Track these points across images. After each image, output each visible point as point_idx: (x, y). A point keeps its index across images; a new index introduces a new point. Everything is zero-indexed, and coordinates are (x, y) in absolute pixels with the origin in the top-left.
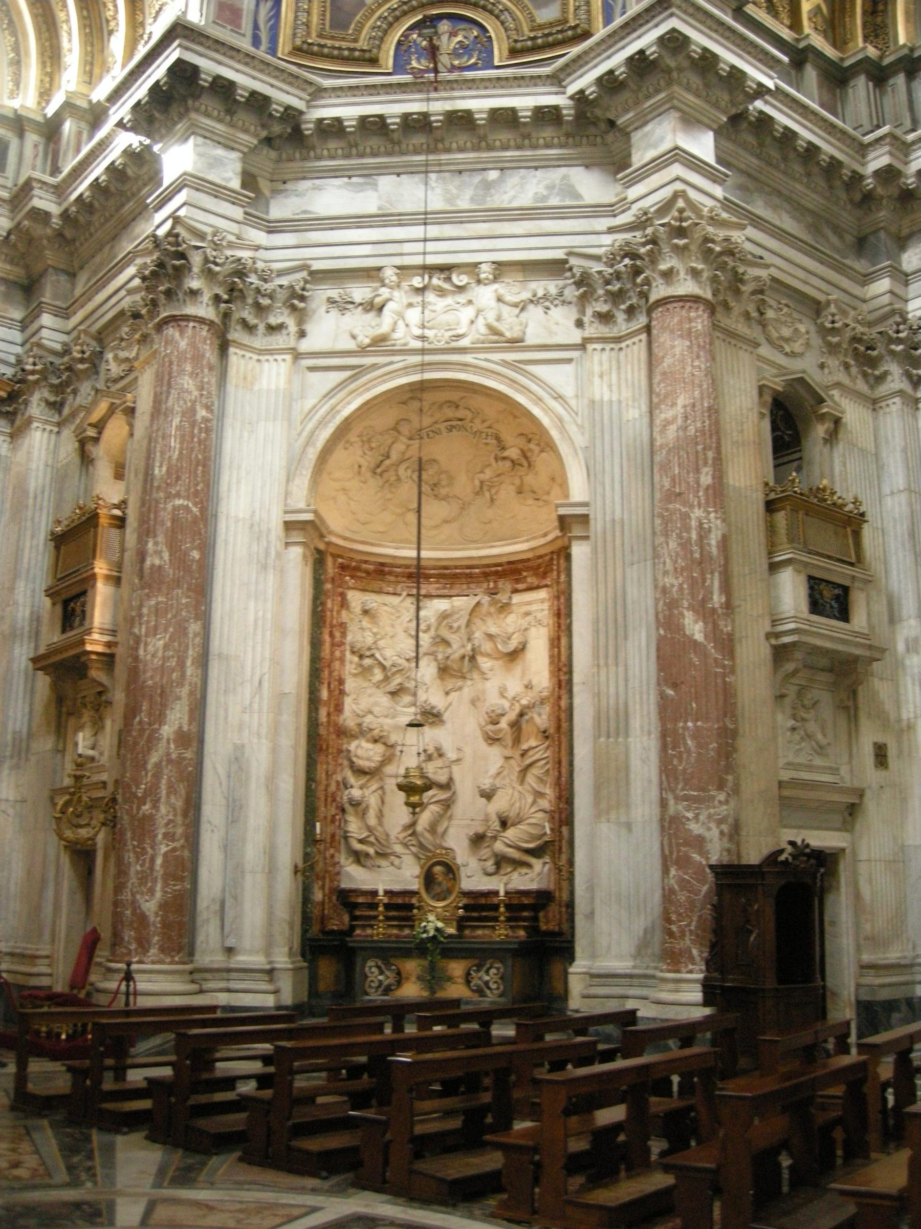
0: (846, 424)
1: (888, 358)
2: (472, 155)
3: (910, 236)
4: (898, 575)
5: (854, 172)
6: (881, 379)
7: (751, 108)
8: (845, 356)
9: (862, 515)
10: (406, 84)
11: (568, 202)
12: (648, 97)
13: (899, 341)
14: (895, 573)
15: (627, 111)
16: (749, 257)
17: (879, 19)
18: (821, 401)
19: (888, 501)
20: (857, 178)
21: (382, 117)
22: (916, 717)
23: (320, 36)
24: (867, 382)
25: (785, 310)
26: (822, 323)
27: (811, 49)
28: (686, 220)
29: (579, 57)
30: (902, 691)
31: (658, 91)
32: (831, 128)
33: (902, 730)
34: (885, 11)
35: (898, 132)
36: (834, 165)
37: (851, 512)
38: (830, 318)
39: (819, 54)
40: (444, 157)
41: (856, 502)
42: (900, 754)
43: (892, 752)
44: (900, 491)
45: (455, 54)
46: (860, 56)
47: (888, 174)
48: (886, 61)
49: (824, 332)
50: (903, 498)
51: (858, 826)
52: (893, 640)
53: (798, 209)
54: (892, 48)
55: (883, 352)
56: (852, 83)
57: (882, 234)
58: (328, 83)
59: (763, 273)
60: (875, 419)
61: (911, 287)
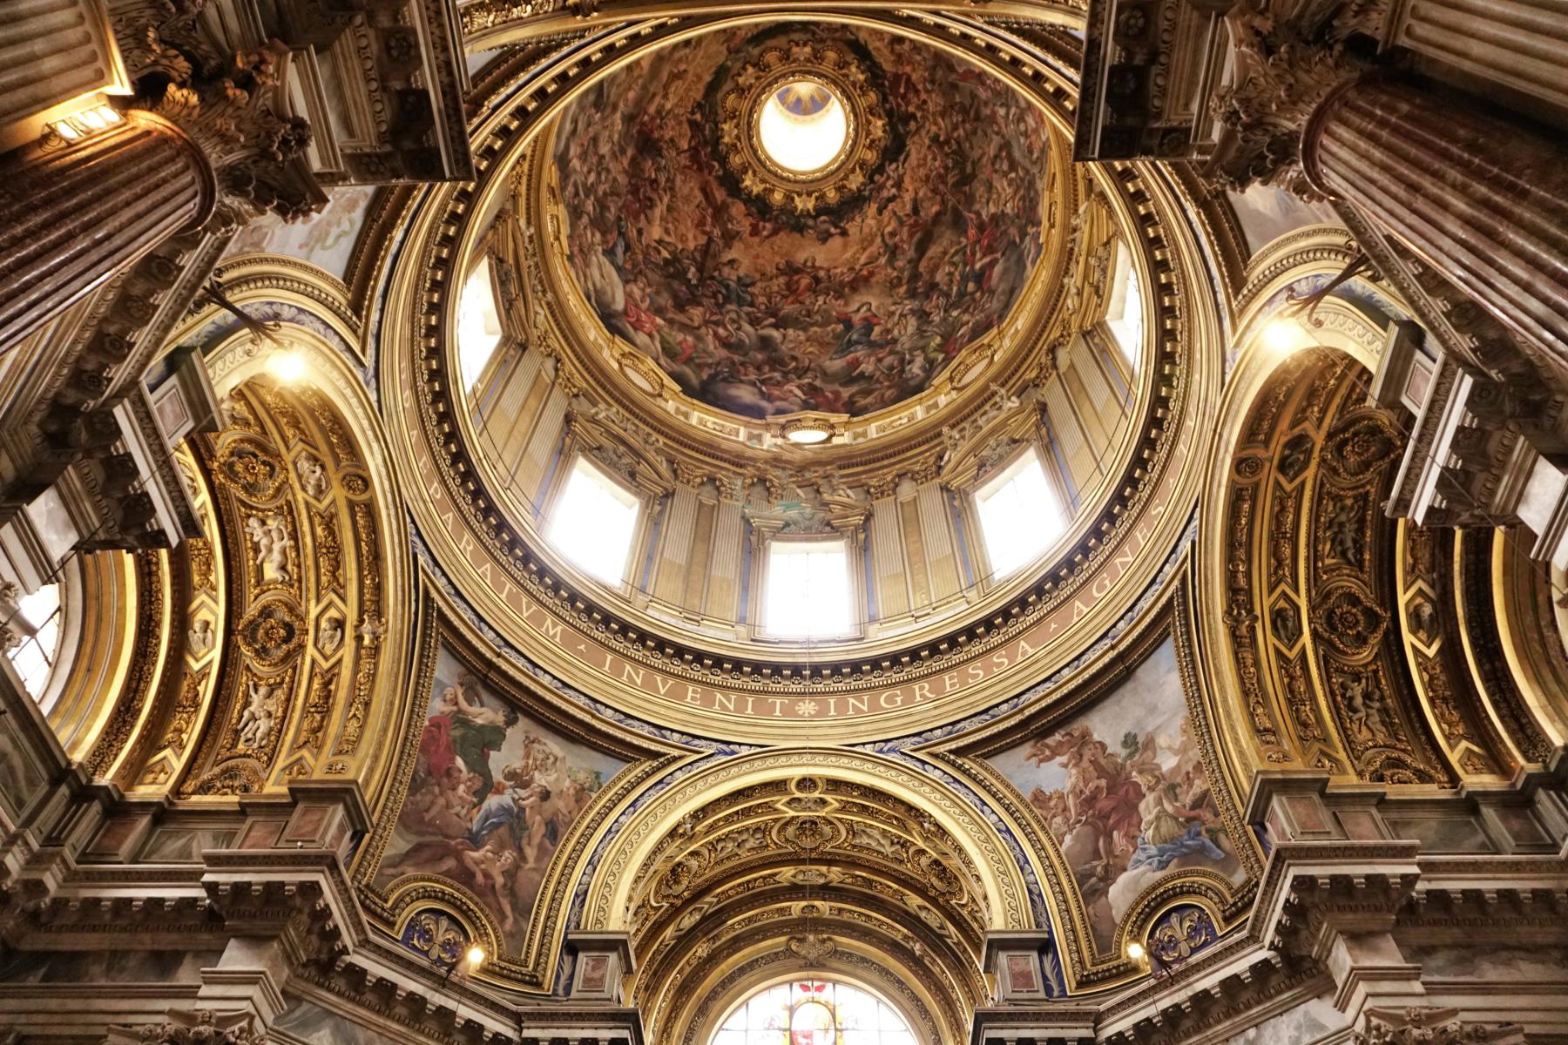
2: (1228, 1023)
10: (1153, 987)
11: (1318, 1037)
12: (1318, 930)
15: (1312, 945)
21: (1148, 1020)
23: (1094, 965)
28: (1386, 1035)
29: (1256, 918)
31: (1321, 924)
39: (1486, 795)
40: (1209, 1033)
45: (1190, 937)
48: (1552, 767)
58: (1102, 1008)
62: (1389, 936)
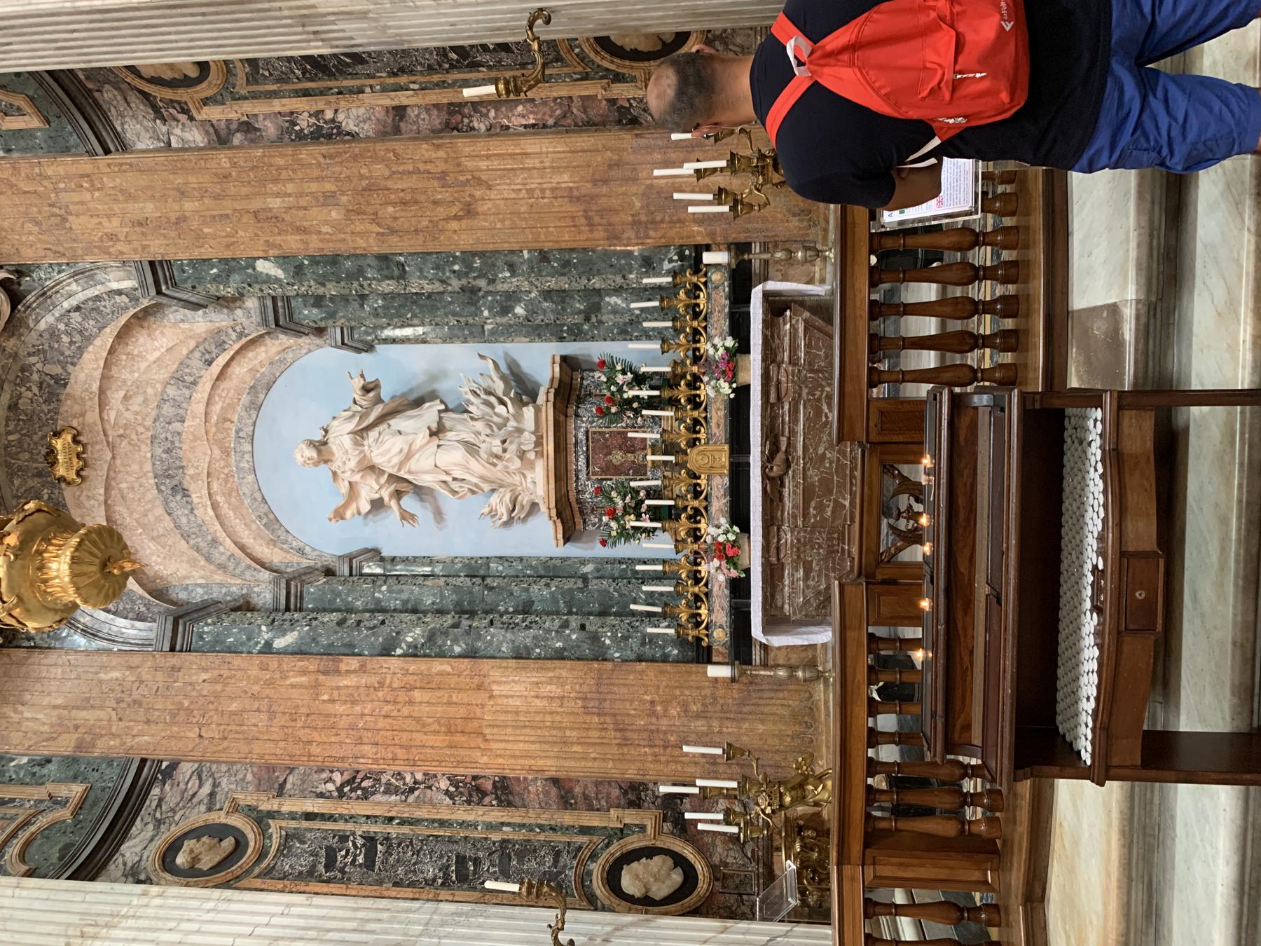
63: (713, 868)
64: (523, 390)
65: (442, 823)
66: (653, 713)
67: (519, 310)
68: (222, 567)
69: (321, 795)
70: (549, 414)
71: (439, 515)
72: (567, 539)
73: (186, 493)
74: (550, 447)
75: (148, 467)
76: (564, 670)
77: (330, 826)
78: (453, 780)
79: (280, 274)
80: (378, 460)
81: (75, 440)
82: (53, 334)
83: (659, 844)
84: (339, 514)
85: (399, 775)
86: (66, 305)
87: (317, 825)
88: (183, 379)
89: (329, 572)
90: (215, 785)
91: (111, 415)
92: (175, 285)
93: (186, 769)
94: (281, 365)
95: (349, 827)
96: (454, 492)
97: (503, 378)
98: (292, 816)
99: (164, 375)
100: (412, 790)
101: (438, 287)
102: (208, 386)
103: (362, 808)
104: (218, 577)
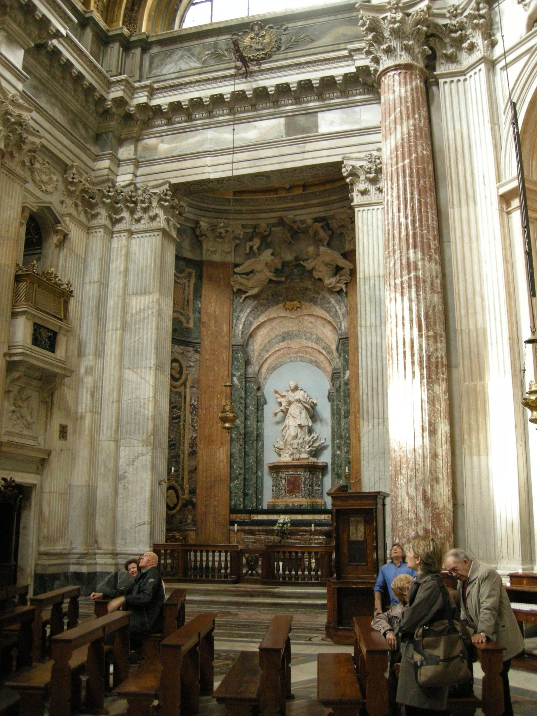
0: (70, 238)
1: (101, 206)
3: (126, 140)
4: (87, 330)
5: (102, 95)
6: (95, 216)
7: (50, 43)
8: (77, 199)
9: (71, 292)
13: (109, 197)
14: (85, 328)
16: (31, 129)
17: (134, 14)
18: (58, 222)
19: (87, 287)
20: (102, 99)
22: (86, 412)
24: (86, 217)
25: (47, 165)
26: (67, 178)
27: (92, 19)
30: (80, 396)
32: (94, 68)
33: (77, 419)
34: (138, 11)
35: (131, 80)
36: (91, 89)
37: (65, 289)
38: (72, 175)
39: (96, 24)
41: (69, 284)
42: (75, 431)
43: (70, 431)
44: (95, 282)
46: (119, 32)
47: (120, 102)
48: (132, 39)
49: (67, 183)
50: (96, 286)
51: (45, 472)
52: (79, 366)
53: (65, 108)
54: (137, 32)
55: (99, 201)
56: (111, 45)
57: (110, 135)
59: (37, 141)
60: (88, 238)
61: (121, 168)
62: (23, 51)
63: (174, 515)
64: (316, 453)
65: (184, 437)
66: (215, 496)
67: (338, 452)
68: (259, 354)
69: (191, 399)
70: (304, 462)
71: (278, 423)
72: (269, 467)
73: (283, 341)
74: (295, 463)
75: (291, 329)
76: (227, 469)
77: (183, 404)
78: (196, 438)
79: (346, 378)
80: (293, 407)
81: (297, 307)
82: (329, 302)
83: (180, 500)
84: (276, 392)
85: (197, 422)
86: (337, 307)
87: (183, 400)
88: (318, 340)
89: (259, 389)
90: (193, 366)
91: (306, 318)
92: (343, 344)
93: (197, 356)
94: (324, 370)
95: (183, 410)
96: (283, 430)
97: (319, 445)
98: (185, 392)
99: (319, 334)
100: (193, 426)
101: (343, 428)
102: (316, 348)
103: (187, 413)
104: (256, 354)
